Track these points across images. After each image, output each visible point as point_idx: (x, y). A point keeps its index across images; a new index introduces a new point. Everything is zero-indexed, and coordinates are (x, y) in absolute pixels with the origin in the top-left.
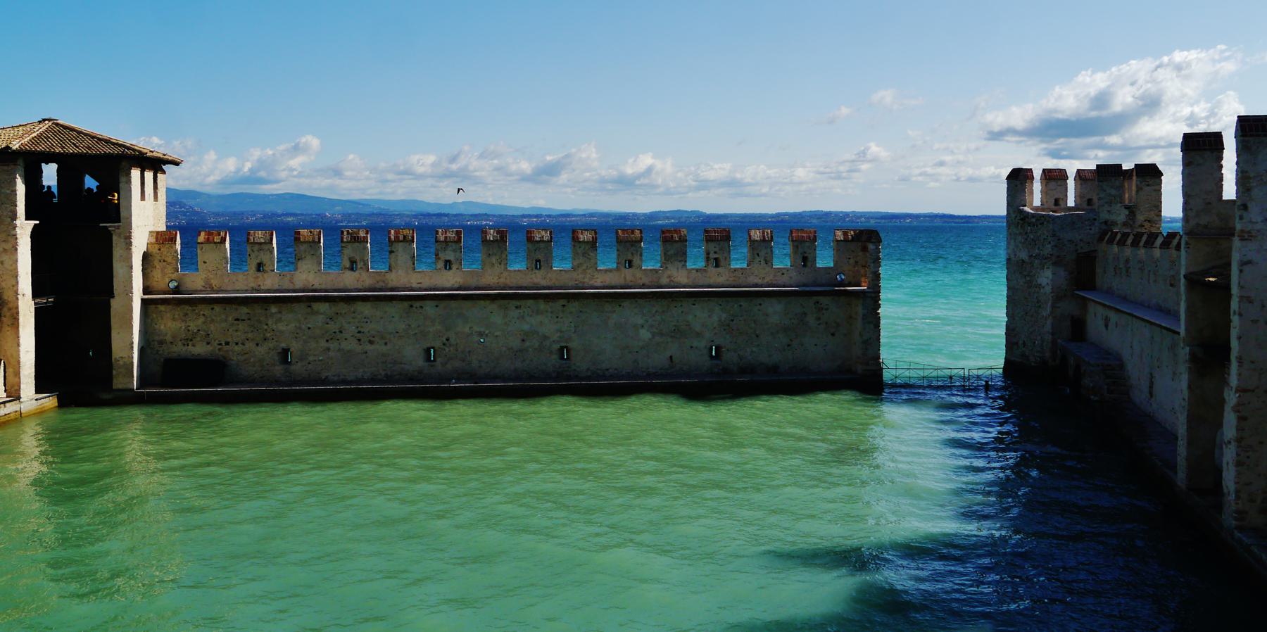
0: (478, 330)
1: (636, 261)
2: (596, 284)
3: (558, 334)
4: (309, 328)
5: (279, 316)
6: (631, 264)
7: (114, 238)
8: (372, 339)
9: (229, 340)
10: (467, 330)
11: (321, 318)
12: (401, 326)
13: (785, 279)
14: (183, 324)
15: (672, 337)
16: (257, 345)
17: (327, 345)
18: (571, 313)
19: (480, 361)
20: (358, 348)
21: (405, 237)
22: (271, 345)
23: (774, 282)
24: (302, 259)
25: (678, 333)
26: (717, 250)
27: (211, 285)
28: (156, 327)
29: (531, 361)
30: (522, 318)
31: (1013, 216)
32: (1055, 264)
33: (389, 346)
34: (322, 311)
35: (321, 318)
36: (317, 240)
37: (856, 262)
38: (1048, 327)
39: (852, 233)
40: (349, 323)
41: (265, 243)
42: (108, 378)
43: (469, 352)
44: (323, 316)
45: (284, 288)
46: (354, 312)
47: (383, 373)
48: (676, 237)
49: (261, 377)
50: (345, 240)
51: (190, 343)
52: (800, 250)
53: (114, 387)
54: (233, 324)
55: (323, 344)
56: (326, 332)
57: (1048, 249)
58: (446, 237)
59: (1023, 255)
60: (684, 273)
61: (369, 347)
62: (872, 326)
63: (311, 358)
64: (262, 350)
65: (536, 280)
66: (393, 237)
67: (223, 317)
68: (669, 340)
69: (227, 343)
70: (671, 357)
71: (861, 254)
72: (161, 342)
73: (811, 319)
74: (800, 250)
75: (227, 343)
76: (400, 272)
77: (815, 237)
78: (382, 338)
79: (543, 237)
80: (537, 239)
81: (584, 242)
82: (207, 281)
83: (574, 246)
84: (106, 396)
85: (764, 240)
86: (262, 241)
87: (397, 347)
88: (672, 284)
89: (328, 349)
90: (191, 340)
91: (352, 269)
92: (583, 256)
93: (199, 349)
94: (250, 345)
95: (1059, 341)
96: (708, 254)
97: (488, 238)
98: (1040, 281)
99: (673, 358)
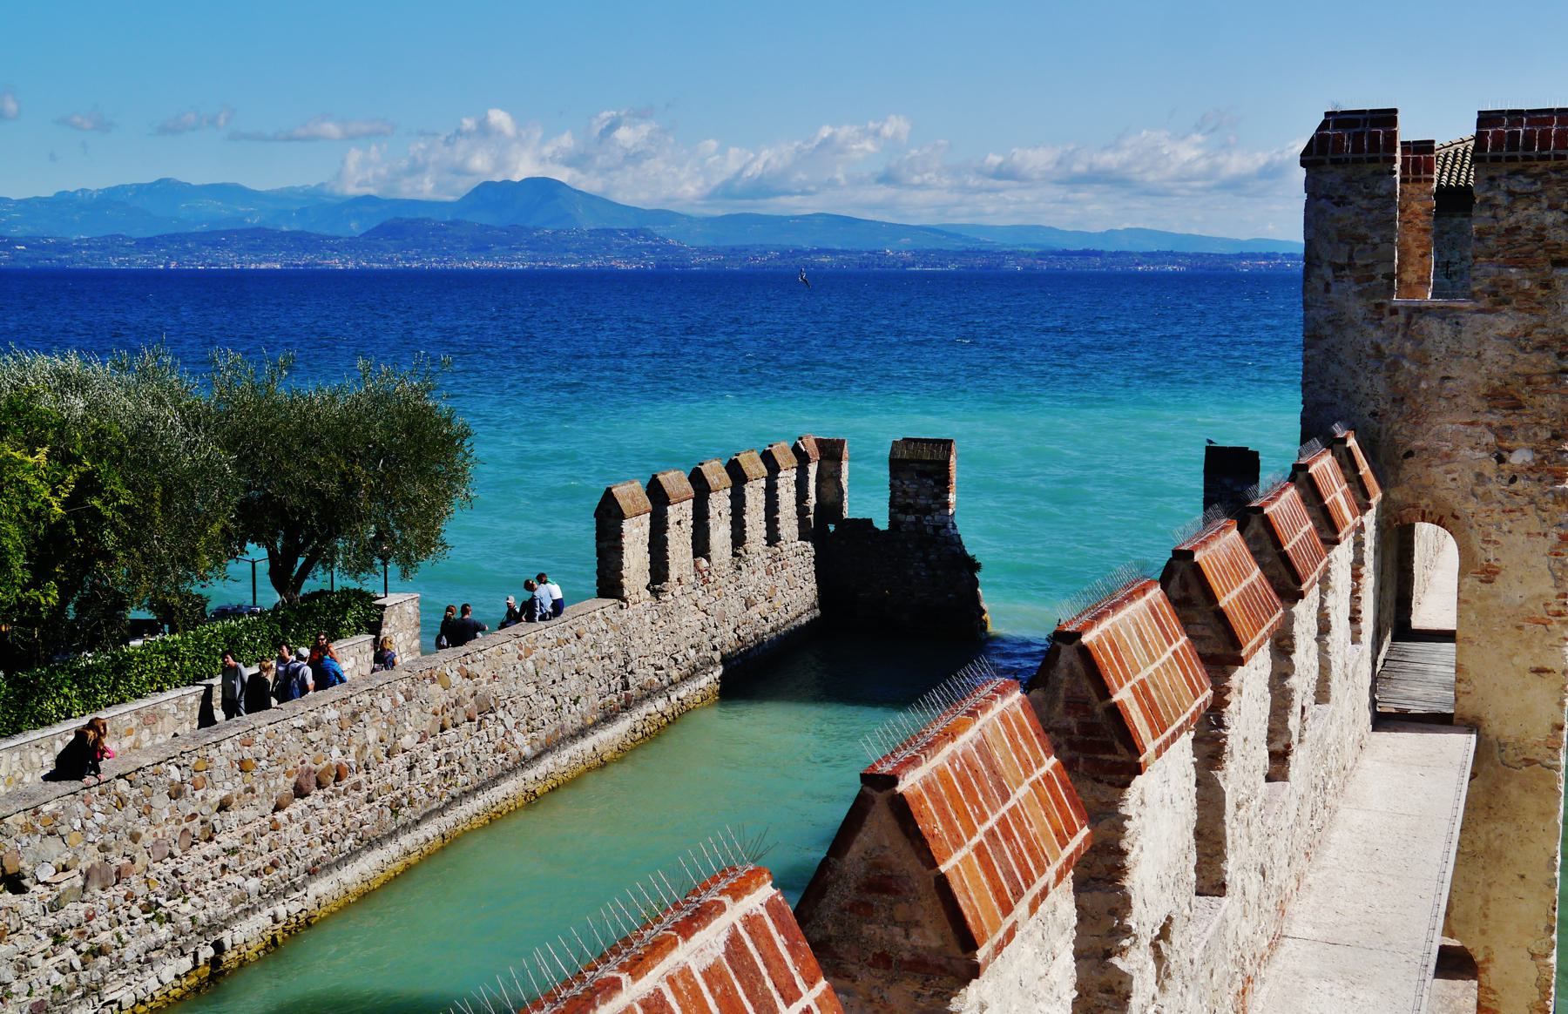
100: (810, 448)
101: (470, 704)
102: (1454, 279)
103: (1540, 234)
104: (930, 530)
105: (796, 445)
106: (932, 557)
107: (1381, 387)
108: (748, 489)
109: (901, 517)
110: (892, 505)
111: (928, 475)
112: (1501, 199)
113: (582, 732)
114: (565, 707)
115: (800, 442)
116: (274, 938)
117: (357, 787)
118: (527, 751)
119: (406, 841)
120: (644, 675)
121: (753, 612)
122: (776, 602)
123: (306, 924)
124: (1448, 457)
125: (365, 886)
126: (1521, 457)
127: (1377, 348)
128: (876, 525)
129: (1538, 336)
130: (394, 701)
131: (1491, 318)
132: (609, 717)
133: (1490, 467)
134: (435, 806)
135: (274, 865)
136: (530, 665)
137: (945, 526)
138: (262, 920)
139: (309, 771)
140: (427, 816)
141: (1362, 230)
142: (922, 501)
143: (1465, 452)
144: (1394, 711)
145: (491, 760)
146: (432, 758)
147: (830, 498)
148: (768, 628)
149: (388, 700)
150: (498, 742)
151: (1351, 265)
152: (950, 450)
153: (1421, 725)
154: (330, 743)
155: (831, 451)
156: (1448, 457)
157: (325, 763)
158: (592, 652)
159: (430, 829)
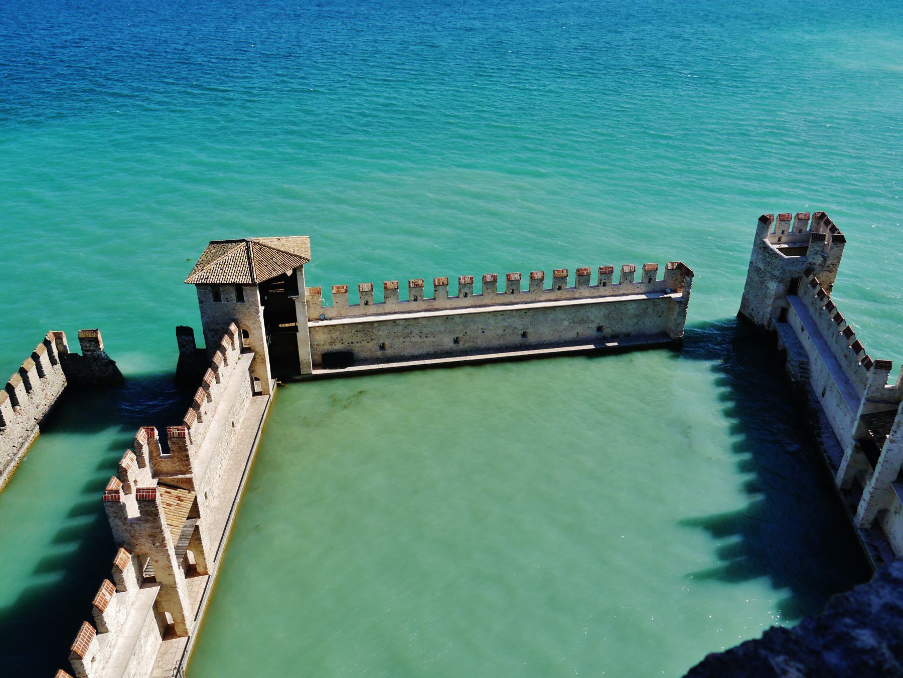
0: (481, 327)
1: (563, 287)
3: (522, 326)
6: (560, 288)
7: (296, 303)
9: (353, 341)
10: (476, 328)
11: (400, 328)
12: (442, 328)
13: (639, 291)
14: (329, 336)
17: (404, 340)
20: (420, 340)
22: (375, 342)
25: (582, 321)
27: (340, 314)
31: (759, 242)
32: (779, 282)
33: (436, 338)
37: (676, 279)
38: (769, 309)
39: (676, 264)
42: (299, 369)
47: (433, 351)
48: (585, 273)
57: (777, 273)
59: (761, 266)
61: (426, 339)
63: (396, 347)
64: (370, 345)
68: (578, 325)
69: (352, 343)
72: (318, 345)
73: (650, 311)
74: (649, 275)
75: (352, 343)
78: (432, 334)
80: (513, 279)
81: (537, 279)
82: (339, 312)
84: (298, 378)
85: (631, 272)
86: (367, 290)
89: (405, 342)
91: (416, 300)
93: (338, 347)
95: (773, 319)
96: (601, 280)
98: (768, 285)
100: (50, 337)
103: (152, 512)
104: (96, 356)
105: (45, 338)
107: (128, 535)
108: (29, 374)
109: (86, 353)
110: (82, 350)
111: (92, 341)
112: (143, 506)
121: (41, 407)
126: (157, 544)
142: (92, 348)
143: (147, 544)
144: (148, 576)
147: (61, 349)
148: (47, 407)
151: (117, 517)
152: (97, 333)
153: (150, 584)
155: (58, 337)
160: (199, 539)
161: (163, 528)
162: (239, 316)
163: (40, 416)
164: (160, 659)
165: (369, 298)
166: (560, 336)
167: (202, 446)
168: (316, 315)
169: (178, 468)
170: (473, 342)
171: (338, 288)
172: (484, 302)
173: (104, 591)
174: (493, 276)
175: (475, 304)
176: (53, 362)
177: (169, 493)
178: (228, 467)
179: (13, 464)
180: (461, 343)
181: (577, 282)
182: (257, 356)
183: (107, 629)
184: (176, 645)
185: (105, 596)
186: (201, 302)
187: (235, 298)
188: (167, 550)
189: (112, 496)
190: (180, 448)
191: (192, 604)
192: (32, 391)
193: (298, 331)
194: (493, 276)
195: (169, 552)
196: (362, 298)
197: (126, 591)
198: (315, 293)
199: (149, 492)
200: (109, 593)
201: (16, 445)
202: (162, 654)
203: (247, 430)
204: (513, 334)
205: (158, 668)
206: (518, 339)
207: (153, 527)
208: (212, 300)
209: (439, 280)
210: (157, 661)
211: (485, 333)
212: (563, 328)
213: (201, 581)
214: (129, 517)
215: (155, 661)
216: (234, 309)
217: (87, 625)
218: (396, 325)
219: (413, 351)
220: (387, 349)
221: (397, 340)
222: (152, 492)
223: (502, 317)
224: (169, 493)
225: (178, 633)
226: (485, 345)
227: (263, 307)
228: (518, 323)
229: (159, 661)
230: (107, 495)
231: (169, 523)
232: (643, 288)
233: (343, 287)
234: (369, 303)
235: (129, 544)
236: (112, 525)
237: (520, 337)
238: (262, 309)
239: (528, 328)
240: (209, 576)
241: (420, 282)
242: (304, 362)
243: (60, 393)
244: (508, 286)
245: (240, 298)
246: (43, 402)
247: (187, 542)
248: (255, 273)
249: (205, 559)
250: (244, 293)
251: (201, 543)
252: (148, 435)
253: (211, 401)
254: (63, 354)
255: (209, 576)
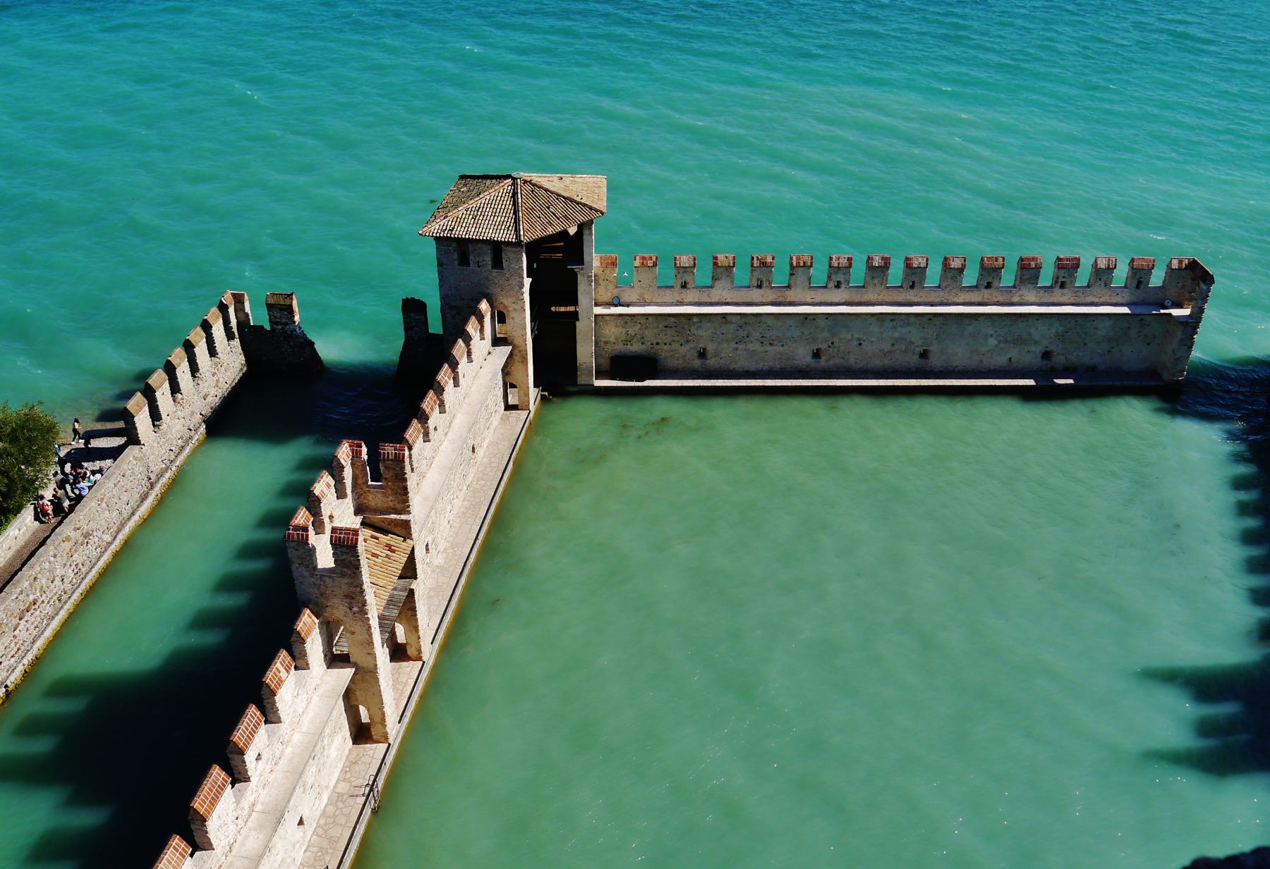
1: (995, 283)
2: (958, 301)
3: (922, 341)
4: (723, 334)
5: (700, 324)
6: (989, 286)
7: (579, 276)
8: (772, 342)
9: (659, 341)
10: (849, 337)
11: (732, 327)
12: (797, 333)
13: (1119, 300)
14: (624, 330)
15: (1014, 344)
16: (681, 345)
18: (935, 325)
19: (856, 359)
20: (762, 349)
21: (804, 263)
22: (692, 346)
23: (1109, 301)
24: (719, 279)
25: (1020, 341)
26: (1064, 275)
28: (603, 331)
29: (897, 359)
30: (894, 328)
33: (784, 348)
34: (734, 321)
35: (732, 327)
36: (732, 265)
37: (1184, 286)
39: (1187, 262)
40: (755, 330)
41: (690, 267)
42: (575, 377)
43: (849, 352)
44: (734, 325)
45: (703, 301)
46: (760, 323)
47: (778, 366)
49: (684, 368)
50: (755, 265)
51: (629, 344)
52: (1138, 276)
53: (579, 383)
54: (662, 330)
55: (733, 345)
56: (737, 336)
58: (839, 263)
60: (1034, 292)
61: (769, 348)
62: (1186, 347)
65: (909, 298)
66: (795, 264)
67: (656, 324)
68: (1012, 346)
69: (658, 344)
70: (1010, 358)
71: (1190, 281)
72: (606, 343)
73: (1133, 333)
74: (1138, 276)
75: (658, 344)
76: (798, 289)
77: (1153, 265)
79: (920, 263)
80: (915, 265)
81: (954, 268)
82: (641, 295)
83: (945, 271)
84: (572, 389)
85: (1108, 268)
86: (687, 265)
87: (791, 348)
88: (1022, 301)
89: (737, 349)
90: (630, 341)
91: (759, 286)
92: (952, 279)
93: (636, 348)
94: (676, 346)
97: (874, 265)
99: (1012, 359)
100: (228, 299)
101: (81, 539)
102: (481, 268)
103: (350, 562)
104: (289, 332)
105: (221, 301)
106: (292, 343)
107: (316, 591)
108: (196, 350)
109: (275, 326)
110: (270, 322)
111: (285, 310)
113: (133, 514)
114: (123, 510)
115: (223, 299)
116: (25, 671)
117: (43, 602)
118: (110, 539)
119: (66, 607)
120: (156, 467)
121: (210, 399)
122: (220, 385)
123: (38, 660)
124: (337, 608)
125: (55, 632)
126: (355, 609)
127: (314, 583)
128: (265, 327)
129: (355, 584)
130: (50, 562)
131: (341, 579)
132: (144, 498)
133: (348, 611)
134: (76, 586)
135: (18, 649)
136: (104, 505)
137: (295, 330)
138: (20, 669)
139: (23, 611)
140: (73, 592)
141: (304, 557)
142: (284, 320)
144: (339, 652)
145: (95, 553)
146: (70, 571)
149: (47, 563)
150: (97, 544)
151: (302, 563)
152: (292, 299)
154: (28, 595)
155: (238, 300)
156: (337, 608)
157: (28, 603)
158: (131, 478)
159: (76, 596)
160: (414, 609)
161: (365, 587)
162: (494, 290)
163: (207, 411)
164: (348, 769)
165: (688, 278)
166: (981, 361)
167: (427, 476)
168: (606, 297)
169: (391, 504)
170: (843, 358)
171: (643, 258)
172: (866, 298)
173: (278, 665)
174: (883, 258)
175: (851, 300)
176: (230, 336)
177: (377, 538)
178: (462, 510)
179: (168, 475)
180: (823, 358)
181: (1018, 278)
182: (516, 351)
183: (279, 717)
184: (372, 752)
185: (279, 672)
186: (440, 264)
187: (490, 263)
188: (368, 619)
189: (298, 534)
190: (396, 476)
191: (397, 700)
192: (198, 375)
193: (578, 320)
194: (883, 258)
195: (370, 622)
196: (679, 276)
197: (309, 668)
198: (608, 264)
199: (349, 534)
200: (285, 669)
201: (173, 449)
202: (351, 763)
203: (493, 459)
204: (906, 351)
205: (344, 780)
206: (913, 360)
207: (350, 585)
208: (456, 263)
209: (798, 258)
210: (343, 771)
211: (863, 347)
212: (988, 348)
213: (410, 668)
214: (319, 567)
215: (341, 771)
216: (487, 279)
217: (217, 770)
218: (727, 322)
219: (747, 364)
220: (709, 357)
221: (725, 345)
222: (353, 535)
223: (891, 324)
224: (377, 538)
225: (374, 737)
226: (860, 365)
227: (530, 280)
228: (915, 335)
229: (346, 772)
230: (291, 532)
231: (373, 581)
232: (1126, 297)
233: (651, 258)
234: (688, 286)
235: (317, 604)
236: (295, 574)
237: (916, 357)
238: (527, 281)
239: (931, 344)
240: (424, 662)
241: (769, 260)
242: (584, 366)
243: (237, 381)
244: (905, 278)
245: (498, 263)
246: (213, 392)
247: (396, 611)
248: (521, 227)
249: (419, 638)
250: (503, 255)
251: (416, 615)
252: (353, 453)
253: (445, 412)
254: (243, 324)
255: (424, 662)
